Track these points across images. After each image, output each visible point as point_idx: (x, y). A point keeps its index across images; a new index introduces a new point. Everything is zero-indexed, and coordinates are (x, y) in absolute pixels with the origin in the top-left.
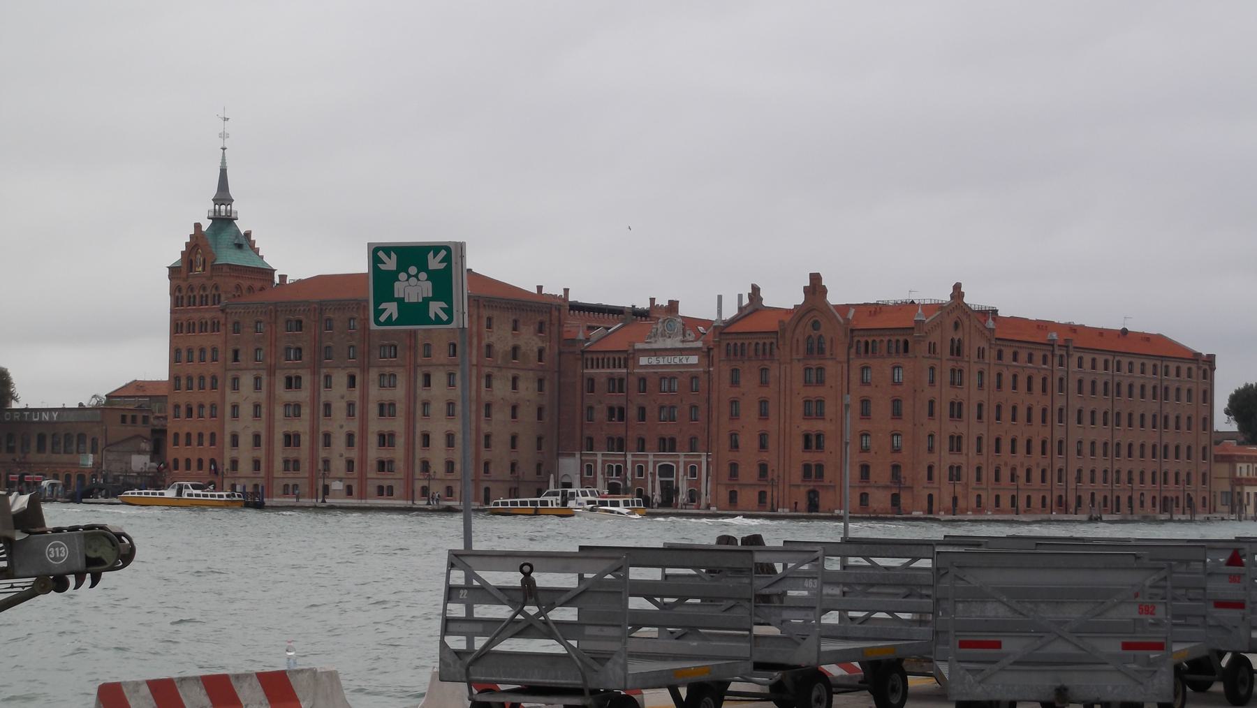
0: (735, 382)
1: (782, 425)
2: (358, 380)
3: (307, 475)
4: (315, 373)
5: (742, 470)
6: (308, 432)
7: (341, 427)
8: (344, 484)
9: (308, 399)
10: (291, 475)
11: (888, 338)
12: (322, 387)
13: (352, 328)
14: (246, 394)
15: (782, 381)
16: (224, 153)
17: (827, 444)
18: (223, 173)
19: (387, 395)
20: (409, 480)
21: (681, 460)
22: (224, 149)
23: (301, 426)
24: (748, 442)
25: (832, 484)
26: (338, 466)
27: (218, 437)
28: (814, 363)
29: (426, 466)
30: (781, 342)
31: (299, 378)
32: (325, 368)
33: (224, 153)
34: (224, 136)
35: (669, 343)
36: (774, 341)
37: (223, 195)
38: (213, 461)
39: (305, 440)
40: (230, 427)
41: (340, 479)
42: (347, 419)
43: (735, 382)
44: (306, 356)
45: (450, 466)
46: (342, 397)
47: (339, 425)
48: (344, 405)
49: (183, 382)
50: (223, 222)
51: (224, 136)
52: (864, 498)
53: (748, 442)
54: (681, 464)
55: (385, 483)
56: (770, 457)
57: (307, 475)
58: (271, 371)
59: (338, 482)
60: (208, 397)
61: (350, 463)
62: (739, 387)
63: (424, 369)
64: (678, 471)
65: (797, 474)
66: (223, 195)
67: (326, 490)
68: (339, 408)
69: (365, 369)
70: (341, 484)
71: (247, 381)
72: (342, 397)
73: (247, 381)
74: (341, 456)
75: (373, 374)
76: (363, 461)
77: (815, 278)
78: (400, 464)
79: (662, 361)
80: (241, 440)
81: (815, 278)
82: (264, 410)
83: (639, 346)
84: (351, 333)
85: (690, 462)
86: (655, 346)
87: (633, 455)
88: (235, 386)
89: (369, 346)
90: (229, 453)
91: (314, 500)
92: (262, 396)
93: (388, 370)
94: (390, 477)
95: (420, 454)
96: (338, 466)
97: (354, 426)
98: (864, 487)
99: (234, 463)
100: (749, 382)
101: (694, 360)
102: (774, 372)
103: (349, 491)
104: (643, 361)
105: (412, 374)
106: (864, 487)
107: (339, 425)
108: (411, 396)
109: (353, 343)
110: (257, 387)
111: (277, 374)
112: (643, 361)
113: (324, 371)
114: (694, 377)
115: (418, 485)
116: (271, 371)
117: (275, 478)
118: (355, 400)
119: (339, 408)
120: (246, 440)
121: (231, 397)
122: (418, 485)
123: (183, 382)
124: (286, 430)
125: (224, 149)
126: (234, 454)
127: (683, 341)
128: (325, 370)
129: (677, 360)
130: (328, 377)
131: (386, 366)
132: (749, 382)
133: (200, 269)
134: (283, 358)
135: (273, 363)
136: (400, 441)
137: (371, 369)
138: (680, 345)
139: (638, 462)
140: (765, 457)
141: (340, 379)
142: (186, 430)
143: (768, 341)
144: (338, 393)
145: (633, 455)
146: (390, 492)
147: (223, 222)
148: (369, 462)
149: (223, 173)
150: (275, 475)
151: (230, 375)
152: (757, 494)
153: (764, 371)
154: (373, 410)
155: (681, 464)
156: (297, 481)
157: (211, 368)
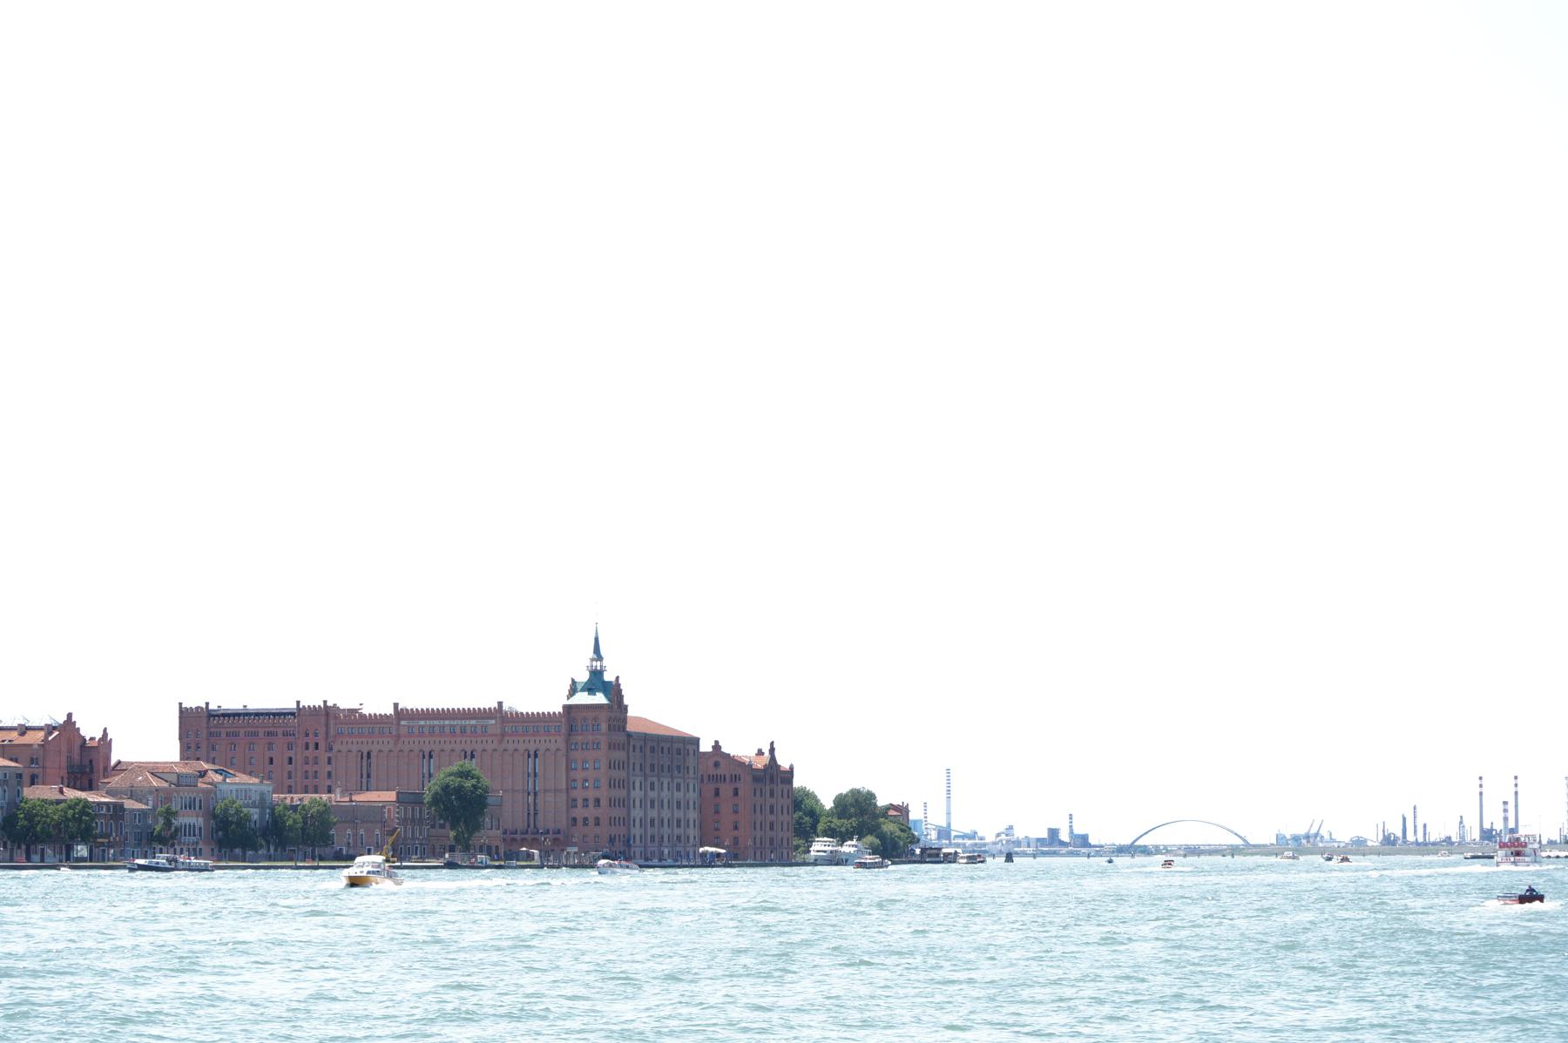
4: (659, 780)
14: (637, 794)
18: (597, 640)
41: (667, 847)
47: (666, 814)
49: (612, 783)
50: (596, 674)
71: (637, 785)
73: (637, 785)
77: (772, 743)
90: (632, 832)
107: (666, 814)
110: (641, 789)
120: (638, 822)
121: (633, 794)
123: (612, 783)
141: (665, 785)
144: (665, 793)
147: (596, 674)
149: (597, 640)
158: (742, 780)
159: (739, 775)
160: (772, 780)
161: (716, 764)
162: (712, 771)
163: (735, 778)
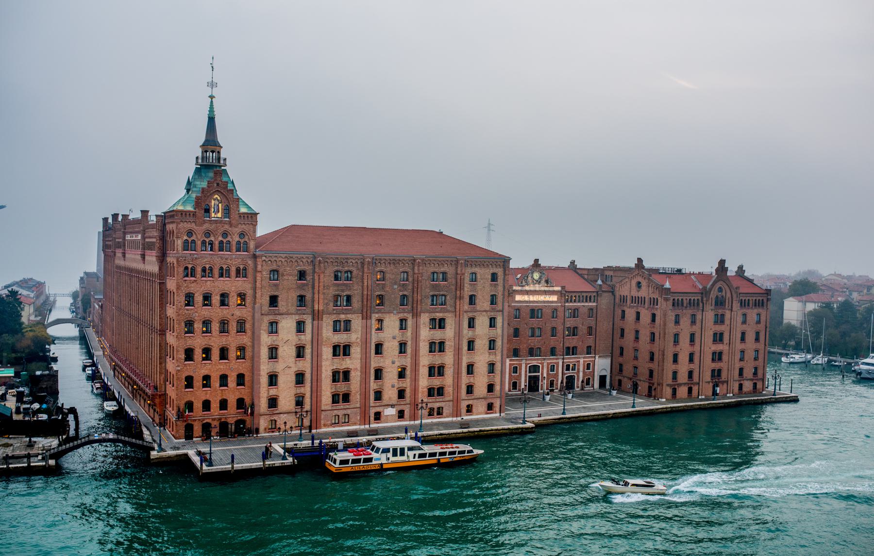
0: (677, 322)
1: (702, 348)
2: (410, 323)
3: (358, 405)
4: (366, 317)
5: (679, 376)
6: (359, 369)
7: (393, 363)
8: (396, 410)
9: (358, 340)
10: (342, 407)
11: (754, 299)
12: (373, 331)
13: (435, 280)
15: (704, 322)
16: (212, 102)
17: (725, 357)
18: (211, 120)
19: (438, 335)
20: (457, 401)
21: (544, 364)
22: (212, 97)
23: (353, 363)
24: (683, 358)
25: (726, 380)
26: (390, 394)
27: (247, 379)
28: (720, 312)
29: (470, 389)
30: (705, 299)
31: (348, 322)
32: (377, 313)
33: (212, 102)
34: (212, 85)
35: (537, 287)
36: (700, 298)
37: (211, 143)
38: (240, 403)
39: (356, 377)
40: (265, 368)
41: (392, 406)
42: (399, 356)
43: (677, 322)
44: (356, 303)
45: (490, 388)
46: (394, 338)
47: (390, 362)
48: (396, 345)
51: (212, 85)
52: (741, 387)
53: (683, 358)
54: (545, 364)
55: (436, 406)
56: (695, 367)
57: (358, 405)
58: (317, 316)
59: (390, 408)
60: (233, 340)
61: (401, 394)
62: (679, 325)
63: (471, 315)
64: (543, 369)
65: (707, 376)
66: (211, 143)
67: (378, 416)
68: (391, 348)
69: (416, 315)
70: (394, 409)
71: (287, 325)
72: (394, 338)
73: (287, 325)
74: (393, 386)
75: (425, 318)
76: (415, 390)
78: (449, 390)
79: (532, 298)
80: (281, 380)
81: (722, 262)
82: (308, 351)
83: (515, 288)
84: (404, 284)
85: (552, 363)
86: (527, 288)
87: (510, 360)
88: (273, 327)
89: (421, 296)
90: (264, 392)
91: (367, 426)
92: (306, 338)
93: (439, 315)
94: (441, 400)
95: (465, 380)
96: (390, 394)
97: (407, 361)
98: (740, 380)
99: (273, 402)
100: (685, 321)
101: (554, 298)
102: (699, 317)
103: (401, 415)
104: (518, 298)
105: (461, 317)
106: (740, 380)
107: (390, 362)
108: (458, 334)
109: (405, 293)
111: (324, 319)
112: (518, 298)
113: (375, 316)
114: (555, 310)
115: (464, 405)
116: (317, 316)
117: (322, 411)
118: (407, 340)
119: (391, 348)
121: (266, 340)
122: (464, 405)
124: (335, 367)
125: (212, 97)
126: (273, 392)
127: (547, 287)
128: (377, 315)
129: (542, 298)
130: (380, 321)
131: (437, 312)
132: (685, 321)
133: (219, 215)
134: (332, 304)
135: (321, 308)
136: (449, 372)
137: (422, 315)
138: (546, 289)
139: (514, 364)
140: (692, 366)
141: (391, 323)
142: (204, 372)
143: (696, 298)
145: (510, 360)
146: (440, 412)
148: (420, 390)
149: (211, 120)
150: (323, 408)
151: (266, 320)
152: (687, 389)
153: (693, 316)
154: (424, 348)
155: (545, 364)
156: (349, 412)
157: (234, 312)
158: (659, 303)
159: (657, 299)
160: (720, 303)
161: (639, 284)
162: (635, 293)
163: (654, 302)
